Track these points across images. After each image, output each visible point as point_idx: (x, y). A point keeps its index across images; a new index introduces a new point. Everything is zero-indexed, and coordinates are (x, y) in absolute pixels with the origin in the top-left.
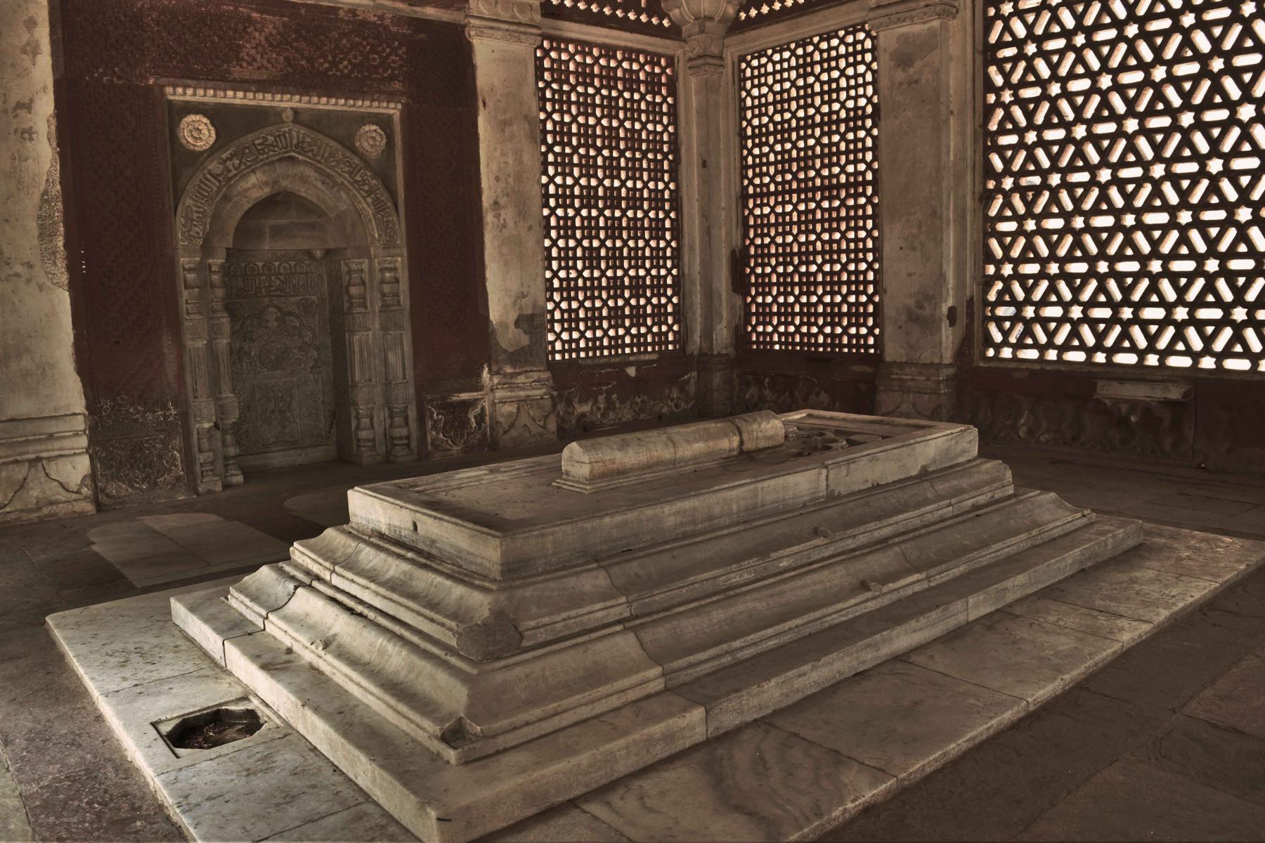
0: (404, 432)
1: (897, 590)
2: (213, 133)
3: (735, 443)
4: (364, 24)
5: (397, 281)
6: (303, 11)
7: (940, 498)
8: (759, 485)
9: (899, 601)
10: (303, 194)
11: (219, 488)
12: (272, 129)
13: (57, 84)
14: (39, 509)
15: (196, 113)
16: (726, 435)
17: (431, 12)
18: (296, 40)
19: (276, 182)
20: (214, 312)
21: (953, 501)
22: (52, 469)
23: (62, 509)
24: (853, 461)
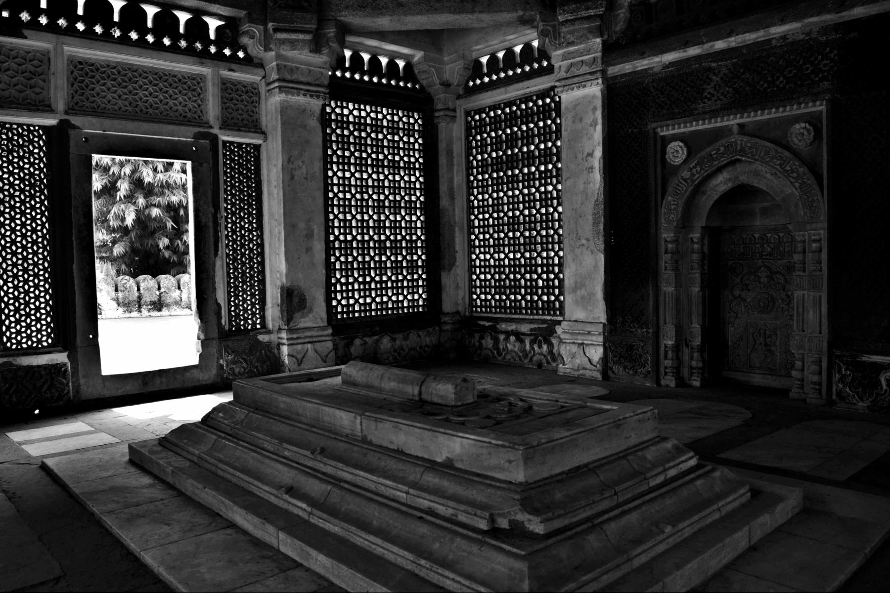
0: (815, 378)
1: (290, 503)
2: (685, 152)
3: (416, 392)
4: (795, 43)
5: (820, 251)
6: (744, 51)
7: (415, 485)
8: (321, 407)
9: (286, 511)
10: (756, 185)
11: (673, 384)
12: (723, 141)
13: (604, 139)
14: (578, 370)
15: (676, 141)
16: (412, 384)
17: (859, 12)
18: (744, 73)
19: (737, 178)
20: (692, 269)
21: (411, 491)
22: (587, 350)
23: (588, 373)
24: (382, 420)
